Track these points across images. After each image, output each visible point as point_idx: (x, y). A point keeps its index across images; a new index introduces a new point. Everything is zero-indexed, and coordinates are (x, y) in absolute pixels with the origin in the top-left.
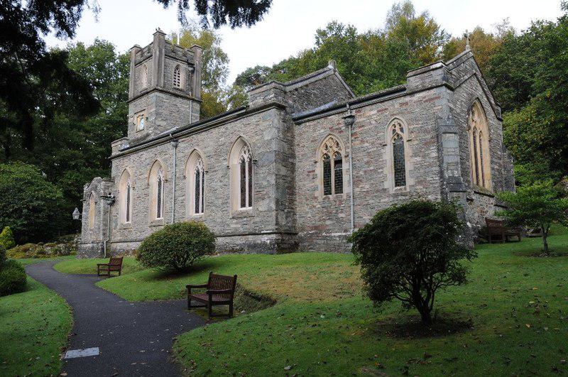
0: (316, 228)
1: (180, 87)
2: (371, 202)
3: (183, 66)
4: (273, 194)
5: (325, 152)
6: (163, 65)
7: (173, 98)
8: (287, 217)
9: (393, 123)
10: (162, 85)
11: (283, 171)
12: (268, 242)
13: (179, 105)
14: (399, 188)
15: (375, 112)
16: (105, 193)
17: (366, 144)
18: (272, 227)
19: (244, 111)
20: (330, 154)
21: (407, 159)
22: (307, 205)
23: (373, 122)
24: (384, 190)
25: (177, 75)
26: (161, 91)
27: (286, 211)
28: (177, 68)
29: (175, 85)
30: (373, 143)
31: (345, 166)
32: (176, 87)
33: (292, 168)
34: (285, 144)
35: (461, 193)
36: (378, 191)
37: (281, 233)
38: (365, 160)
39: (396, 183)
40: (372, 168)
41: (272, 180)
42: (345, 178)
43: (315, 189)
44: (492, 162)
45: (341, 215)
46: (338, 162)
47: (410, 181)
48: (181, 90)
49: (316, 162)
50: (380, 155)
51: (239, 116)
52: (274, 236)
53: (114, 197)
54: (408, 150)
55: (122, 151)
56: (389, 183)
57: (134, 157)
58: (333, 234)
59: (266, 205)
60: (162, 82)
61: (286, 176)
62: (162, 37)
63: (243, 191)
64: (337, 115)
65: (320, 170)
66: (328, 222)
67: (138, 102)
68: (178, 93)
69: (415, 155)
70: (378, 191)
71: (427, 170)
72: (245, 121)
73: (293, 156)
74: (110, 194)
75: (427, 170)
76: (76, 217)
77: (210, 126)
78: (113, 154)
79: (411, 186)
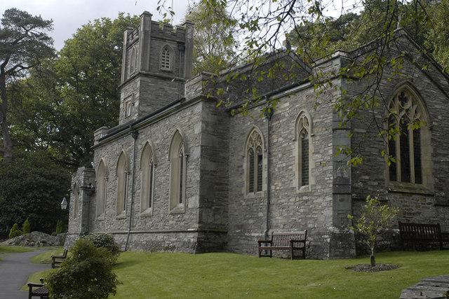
0: (241, 227)
1: (169, 69)
2: (282, 201)
3: (173, 46)
4: (195, 188)
5: (251, 146)
6: (149, 47)
7: (160, 82)
8: (214, 215)
9: (301, 117)
10: (148, 69)
11: (211, 166)
12: (192, 240)
13: (167, 88)
14: (303, 187)
15: (287, 104)
16: (85, 183)
17: (280, 139)
18: (196, 226)
19: (179, 104)
20: (254, 149)
21: (310, 155)
22: (236, 202)
23: (287, 115)
24: (293, 188)
25: (166, 56)
26: (146, 75)
27: (213, 208)
28: (166, 48)
29: (164, 66)
30: (285, 138)
31: (265, 162)
32: (164, 69)
33: (225, 161)
34: (215, 137)
35: (346, 196)
36: (286, 190)
37: (205, 232)
38: (280, 155)
39: (303, 181)
40: (284, 165)
41: (197, 176)
42: (265, 174)
43: (242, 185)
44: (435, 155)
45: (261, 214)
46: (260, 158)
47: (312, 180)
48: (169, 72)
49: (244, 157)
50: (290, 151)
51: (177, 108)
52: (196, 234)
53: (94, 188)
54: (311, 148)
55: (99, 140)
56: (296, 182)
57: (109, 147)
58: (253, 234)
59: (194, 202)
60: (148, 65)
61: (214, 172)
62: (147, 18)
63: (181, 186)
64: (260, 107)
65: (246, 165)
66: (251, 221)
67: (127, 87)
68: (165, 75)
69: (316, 152)
70: (286, 190)
71: (325, 169)
72: (181, 114)
73: (225, 147)
74: (90, 185)
75: (325, 169)
76: (64, 207)
77: (159, 118)
78: (96, 143)
79: (312, 186)
